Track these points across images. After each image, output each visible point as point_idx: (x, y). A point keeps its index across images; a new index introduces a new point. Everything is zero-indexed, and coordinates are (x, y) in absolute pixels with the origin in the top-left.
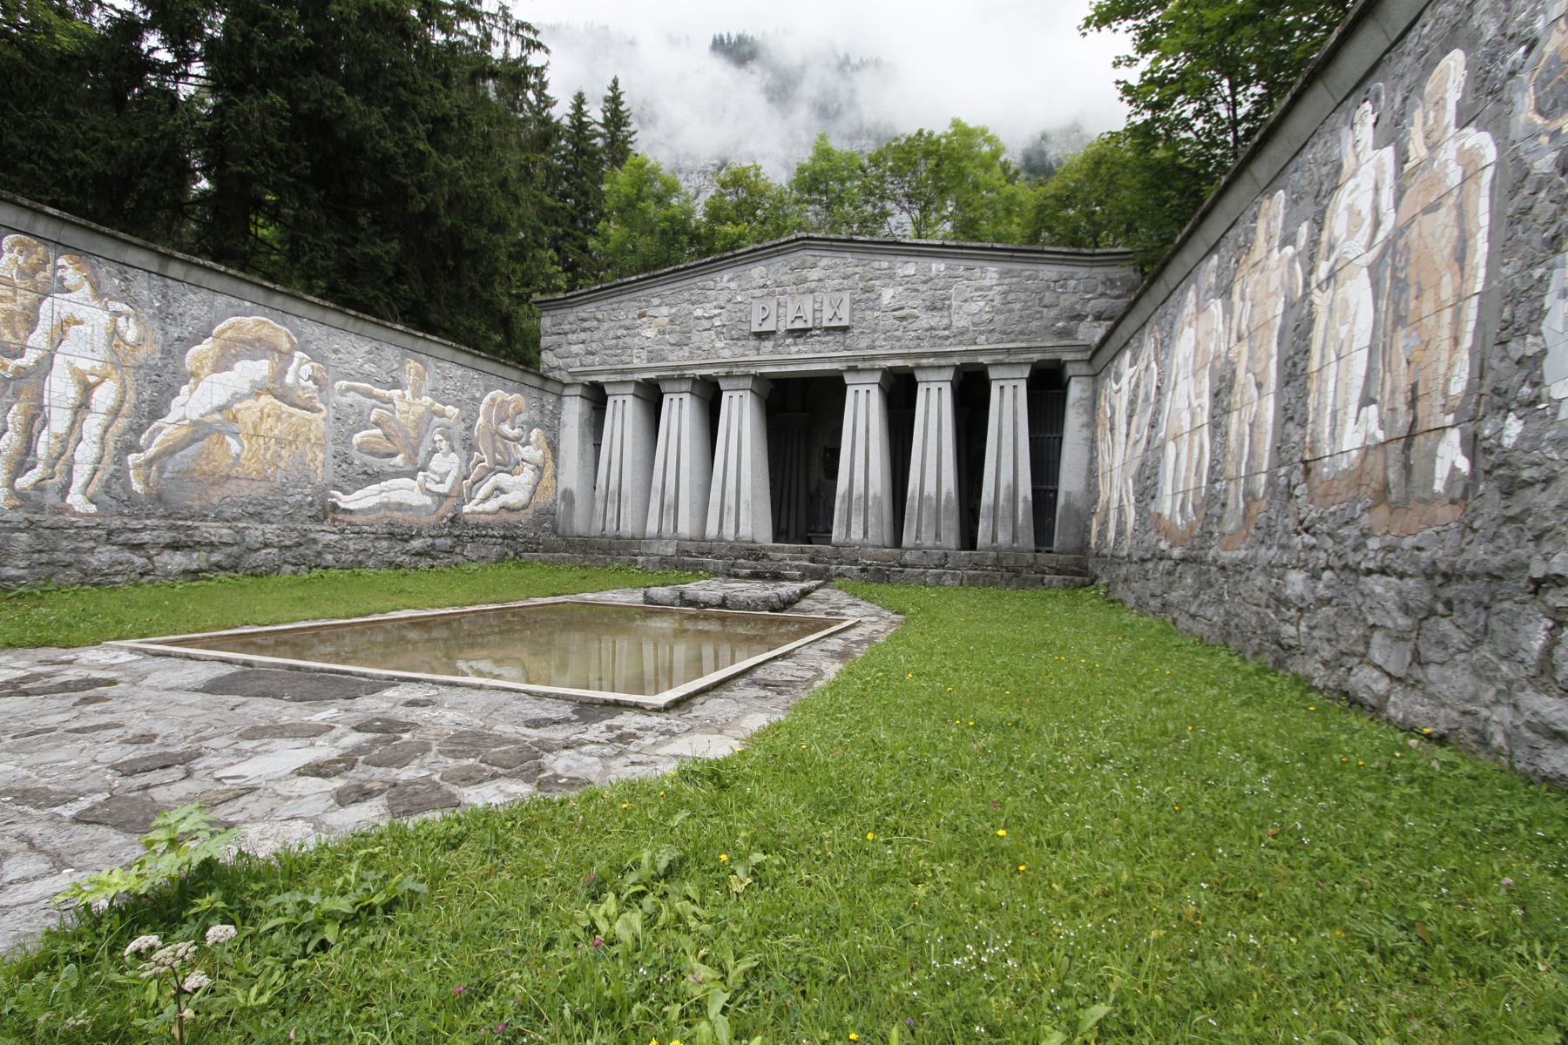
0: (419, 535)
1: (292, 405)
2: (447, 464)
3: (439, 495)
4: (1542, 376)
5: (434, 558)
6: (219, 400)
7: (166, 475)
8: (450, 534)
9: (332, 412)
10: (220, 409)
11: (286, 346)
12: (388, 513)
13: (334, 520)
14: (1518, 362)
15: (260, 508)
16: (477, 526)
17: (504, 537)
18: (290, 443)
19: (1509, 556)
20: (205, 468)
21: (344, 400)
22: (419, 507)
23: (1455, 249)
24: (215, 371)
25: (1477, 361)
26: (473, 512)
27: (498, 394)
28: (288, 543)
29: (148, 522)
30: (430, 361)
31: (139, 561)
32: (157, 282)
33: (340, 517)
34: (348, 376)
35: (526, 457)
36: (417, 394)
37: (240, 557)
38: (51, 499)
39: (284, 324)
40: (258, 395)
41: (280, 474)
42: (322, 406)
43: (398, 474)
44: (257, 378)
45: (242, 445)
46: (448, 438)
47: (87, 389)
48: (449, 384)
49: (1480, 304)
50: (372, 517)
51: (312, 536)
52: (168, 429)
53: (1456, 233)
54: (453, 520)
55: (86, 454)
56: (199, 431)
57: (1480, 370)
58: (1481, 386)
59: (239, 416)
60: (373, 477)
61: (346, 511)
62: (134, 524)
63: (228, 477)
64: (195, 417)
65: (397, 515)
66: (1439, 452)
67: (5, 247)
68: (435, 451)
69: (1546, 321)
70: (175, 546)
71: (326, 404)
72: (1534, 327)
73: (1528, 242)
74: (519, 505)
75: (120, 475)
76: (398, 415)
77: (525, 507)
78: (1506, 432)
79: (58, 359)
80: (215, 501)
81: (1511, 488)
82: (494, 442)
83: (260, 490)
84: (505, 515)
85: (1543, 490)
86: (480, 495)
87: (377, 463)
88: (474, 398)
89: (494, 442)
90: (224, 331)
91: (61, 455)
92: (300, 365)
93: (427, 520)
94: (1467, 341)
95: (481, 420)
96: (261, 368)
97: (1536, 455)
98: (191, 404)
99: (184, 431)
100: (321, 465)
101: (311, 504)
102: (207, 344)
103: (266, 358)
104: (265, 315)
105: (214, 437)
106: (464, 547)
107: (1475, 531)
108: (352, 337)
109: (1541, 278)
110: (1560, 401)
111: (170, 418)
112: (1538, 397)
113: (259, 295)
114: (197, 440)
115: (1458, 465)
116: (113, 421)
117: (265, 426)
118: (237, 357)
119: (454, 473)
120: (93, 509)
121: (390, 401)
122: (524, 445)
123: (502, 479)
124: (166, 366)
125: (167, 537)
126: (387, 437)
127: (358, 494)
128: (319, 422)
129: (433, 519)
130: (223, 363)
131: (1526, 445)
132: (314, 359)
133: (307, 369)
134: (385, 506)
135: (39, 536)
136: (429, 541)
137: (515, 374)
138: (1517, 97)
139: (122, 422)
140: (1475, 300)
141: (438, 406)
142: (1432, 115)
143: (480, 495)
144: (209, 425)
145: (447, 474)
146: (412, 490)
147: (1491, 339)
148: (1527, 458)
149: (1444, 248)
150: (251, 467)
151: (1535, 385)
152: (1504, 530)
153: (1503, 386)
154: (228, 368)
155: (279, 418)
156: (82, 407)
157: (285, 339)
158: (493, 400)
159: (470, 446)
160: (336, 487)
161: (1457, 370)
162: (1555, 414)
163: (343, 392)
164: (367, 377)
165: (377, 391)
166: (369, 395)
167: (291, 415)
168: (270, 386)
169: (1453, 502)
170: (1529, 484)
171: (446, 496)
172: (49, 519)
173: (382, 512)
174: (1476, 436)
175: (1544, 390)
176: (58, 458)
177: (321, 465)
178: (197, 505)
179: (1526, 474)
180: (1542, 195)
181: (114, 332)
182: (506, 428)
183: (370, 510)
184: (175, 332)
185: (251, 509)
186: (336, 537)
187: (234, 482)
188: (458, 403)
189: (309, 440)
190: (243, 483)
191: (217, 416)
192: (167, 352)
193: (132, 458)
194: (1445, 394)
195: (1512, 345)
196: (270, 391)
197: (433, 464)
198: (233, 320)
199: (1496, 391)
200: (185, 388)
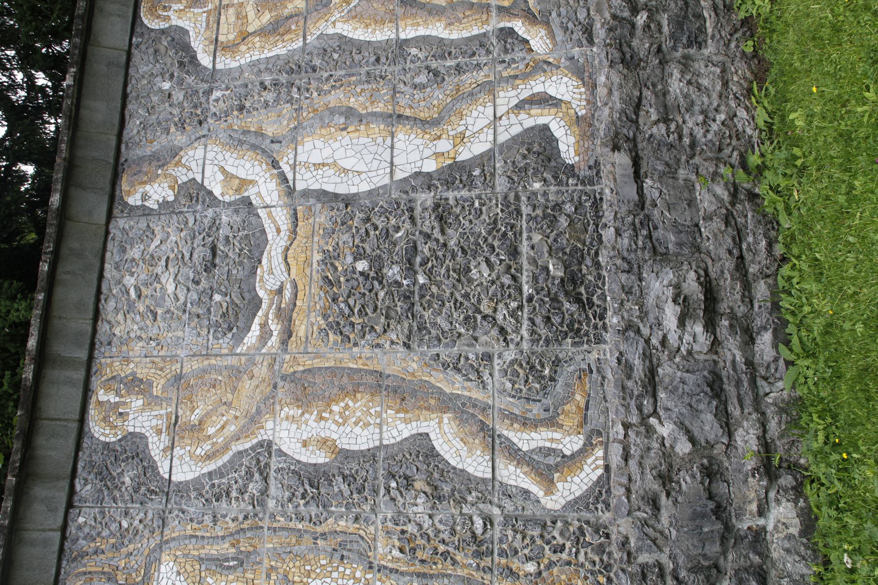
67: (163, 25)
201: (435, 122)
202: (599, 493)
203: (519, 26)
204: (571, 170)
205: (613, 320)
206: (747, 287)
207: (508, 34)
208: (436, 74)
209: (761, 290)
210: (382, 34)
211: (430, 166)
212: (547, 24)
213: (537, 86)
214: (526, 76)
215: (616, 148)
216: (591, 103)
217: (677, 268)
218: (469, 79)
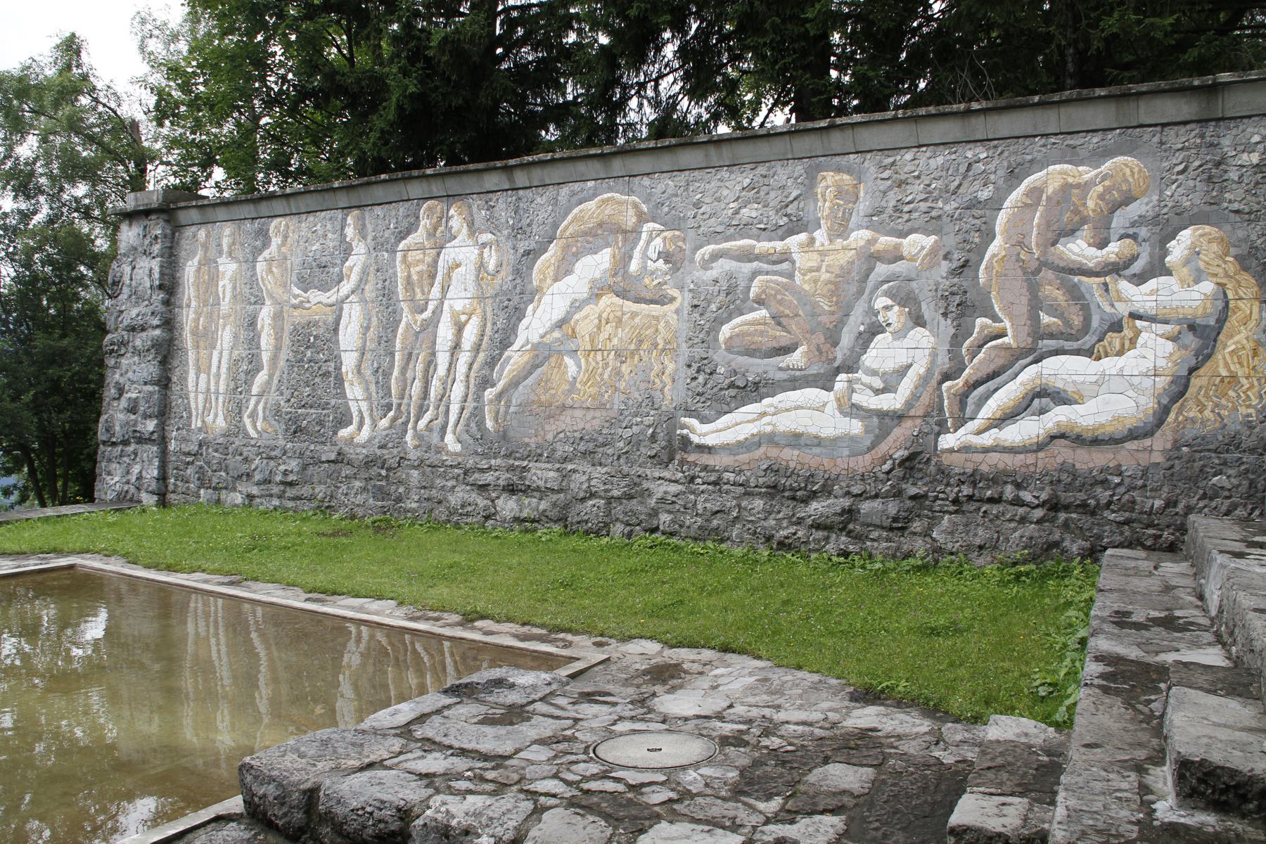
0: (826, 491)
1: (638, 300)
2: (905, 354)
3: (882, 415)
5: (859, 538)
6: (558, 315)
7: (512, 409)
8: (898, 494)
9: (688, 296)
10: (560, 324)
11: (630, 220)
12: (773, 452)
13: (683, 462)
15: (591, 445)
16: (974, 478)
17: (1054, 506)
18: (632, 354)
20: (543, 398)
21: (712, 274)
22: (835, 441)
24: (556, 279)
26: (966, 449)
27: (1053, 176)
28: (616, 493)
29: (493, 462)
30: (870, 164)
31: (482, 502)
32: (511, 197)
33: (691, 458)
34: (715, 236)
35: (1148, 306)
36: (841, 229)
37: (566, 507)
38: (435, 439)
39: (630, 192)
40: (598, 296)
41: (618, 399)
42: (675, 292)
43: (795, 383)
44: (597, 275)
45: (579, 367)
46: (906, 299)
47: (460, 328)
48: (916, 189)
50: (744, 457)
51: (645, 485)
52: (515, 358)
54: (911, 464)
55: (457, 391)
56: (542, 355)
59: (577, 330)
60: (754, 390)
61: (702, 448)
62: (484, 464)
63: (564, 408)
64: (535, 338)
65: (790, 456)
68: (875, 330)
70: (511, 489)
71: (681, 288)
74: (1120, 429)
75: (478, 413)
76: (798, 277)
77: (1133, 435)
79: (446, 307)
80: (550, 437)
82: (1033, 289)
83: (593, 422)
84: (1063, 453)
86: (991, 408)
87: (756, 367)
88: (974, 204)
89: (1033, 289)
90: (567, 227)
91: (443, 396)
92: (648, 243)
93: (842, 463)
95: (996, 247)
96: (597, 263)
98: (535, 325)
99: (526, 358)
100: (670, 380)
101: (653, 438)
102: (553, 248)
103: (608, 245)
104: (610, 189)
105: (553, 360)
106: (934, 521)
108: (724, 173)
111: (516, 347)
113: (595, 167)
114: (538, 366)
116: (476, 357)
117: (604, 335)
118: (577, 256)
119: (919, 369)
120: (458, 448)
121: (785, 257)
122: (1139, 279)
123: (1062, 369)
124: (515, 287)
125: (504, 478)
126: (777, 319)
127: (726, 419)
128: (670, 318)
129: (863, 463)
130: (563, 270)
132: (668, 226)
133: (658, 243)
134: (770, 439)
135: (424, 474)
136: (846, 502)
137: (1097, 115)
139: (481, 356)
141: (885, 241)
143: (991, 408)
144: (549, 347)
145: (903, 371)
146: (821, 408)
150: (586, 393)
154: (568, 272)
155: (619, 321)
156: (456, 347)
157: (631, 212)
158: (1035, 193)
159: (963, 306)
160: (690, 413)
163: (706, 265)
164: (744, 229)
165: (763, 246)
166: (747, 256)
167: (634, 315)
168: (611, 281)
171: (899, 417)
172: (433, 458)
173: (762, 449)
176: (441, 400)
177: (670, 380)
178: (532, 442)
181: (481, 266)
182: (1079, 249)
183: (743, 446)
184: (523, 246)
185: (582, 447)
186: (674, 488)
187: (569, 412)
188: (933, 224)
189: (656, 345)
190: (578, 413)
191: (557, 334)
192: (517, 272)
193: (489, 393)
196: (612, 289)
197: (870, 358)
198: (576, 211)
200: (530, 308)
201: (359, 372)
202: (247, 435)
203: (391, 414)
204: (335, 433)
205: (289, 445)
206: (293, 499)
207: (389, 407)
208: (377, 371)
209: (290, 504)
210: (398, 345)
211: (344, 370)
212: (390, 427)
213: (367, 421)
214: (371, 415)
215: (339, 454)
216: (358, 445)
217: (298, 473)
218: (373, 387)
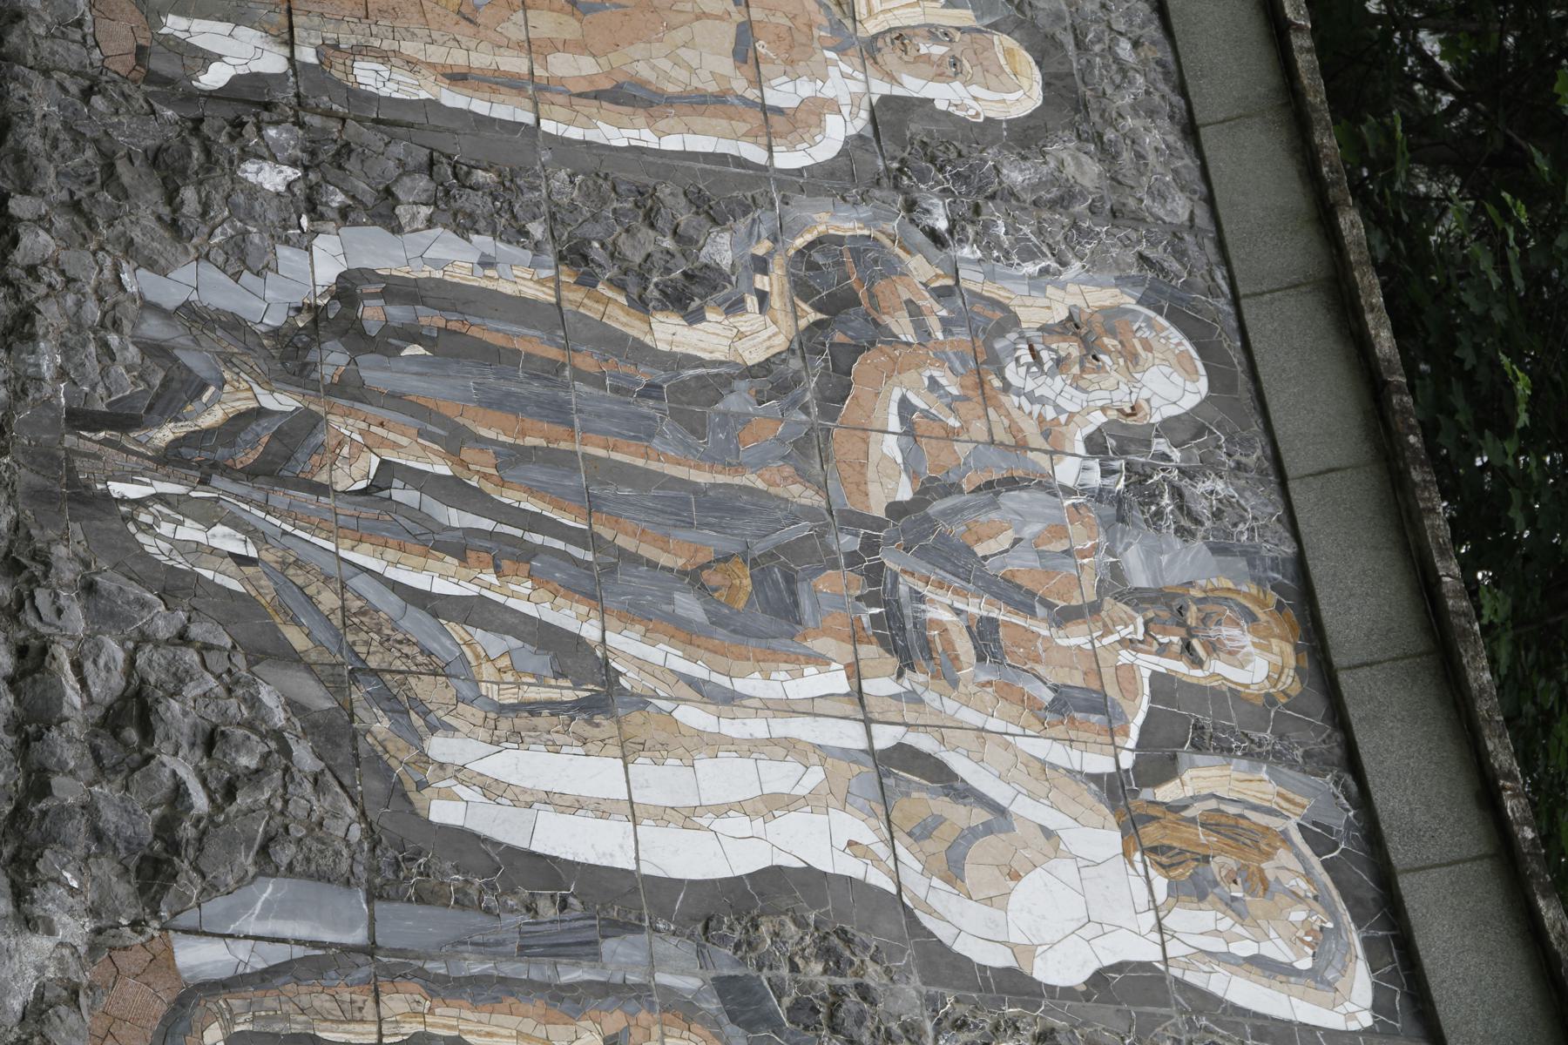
4: (355, 224)
14: (388, 191)
19: (43, 162)
23: (641, 84)
25: (409, 117)
49: (517, 126)
53: (671, 89)
57: (392, 119)
58: (359, 121)
66: (244, 32)
69: (449, 234)
72: (448, 218)
73: (595, 218)
78: (266, 166)
81: (166, 169)
85: (159, 218)
94: (453, 99)
97: (220, 212)
107: (87, 94)
109: (526, 234)
110: (309, 249)
112: (322, 217)
115: (215, 67)
131: (240, 199)
138: (865, 211)
140: (527, 118)
142: (938, 50)
147: (445, 143)
148: (217, 198)
149: (652, 64)
151: (344, 214)
152: (89, 153)
153: (352, 164)
161: (406, 78)
162: (287, 242)
169: (141, 53)
170: (171, 196)
174: (268, 106)
175: (331, 226)
179: (189, 194)
180: (668, 243)
194: (360, 51)
195: (423, 182)
199: (346, 149)
